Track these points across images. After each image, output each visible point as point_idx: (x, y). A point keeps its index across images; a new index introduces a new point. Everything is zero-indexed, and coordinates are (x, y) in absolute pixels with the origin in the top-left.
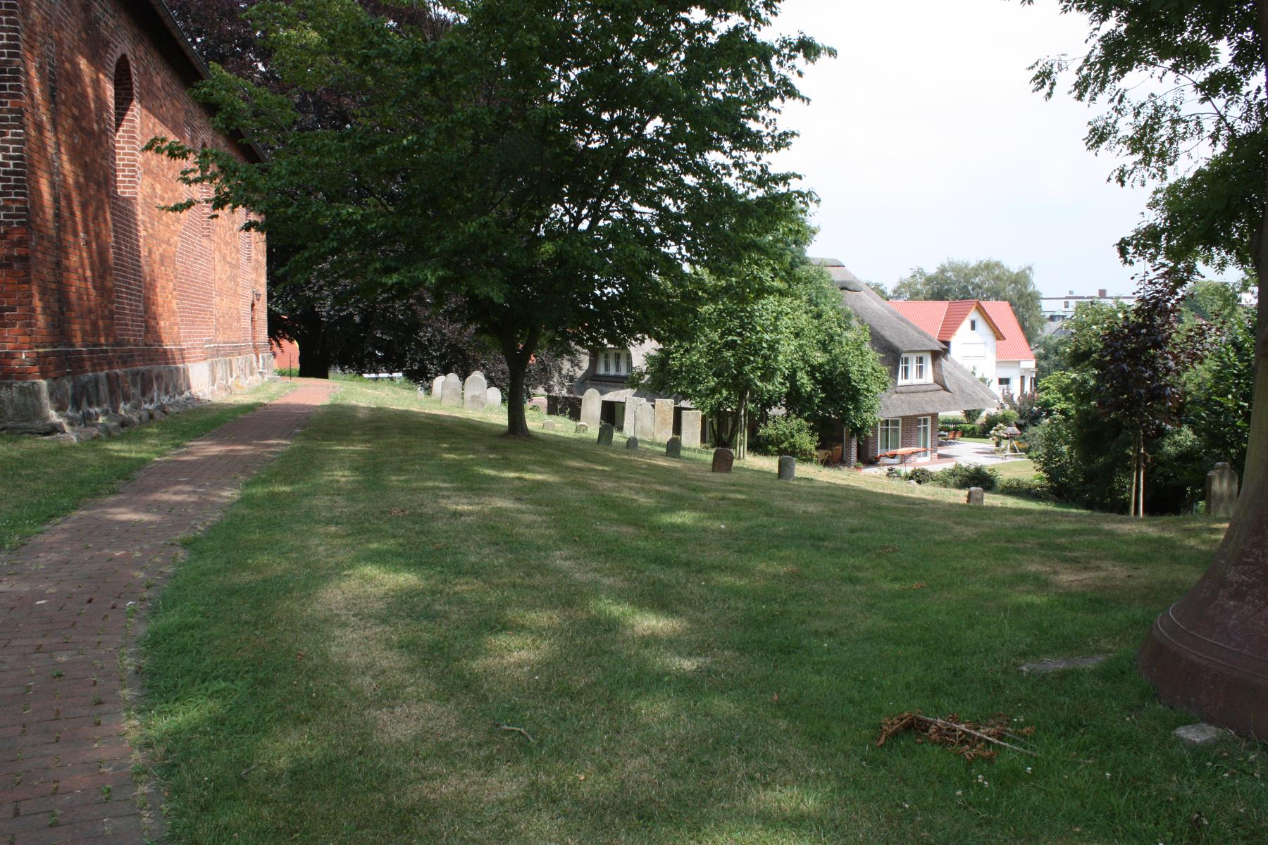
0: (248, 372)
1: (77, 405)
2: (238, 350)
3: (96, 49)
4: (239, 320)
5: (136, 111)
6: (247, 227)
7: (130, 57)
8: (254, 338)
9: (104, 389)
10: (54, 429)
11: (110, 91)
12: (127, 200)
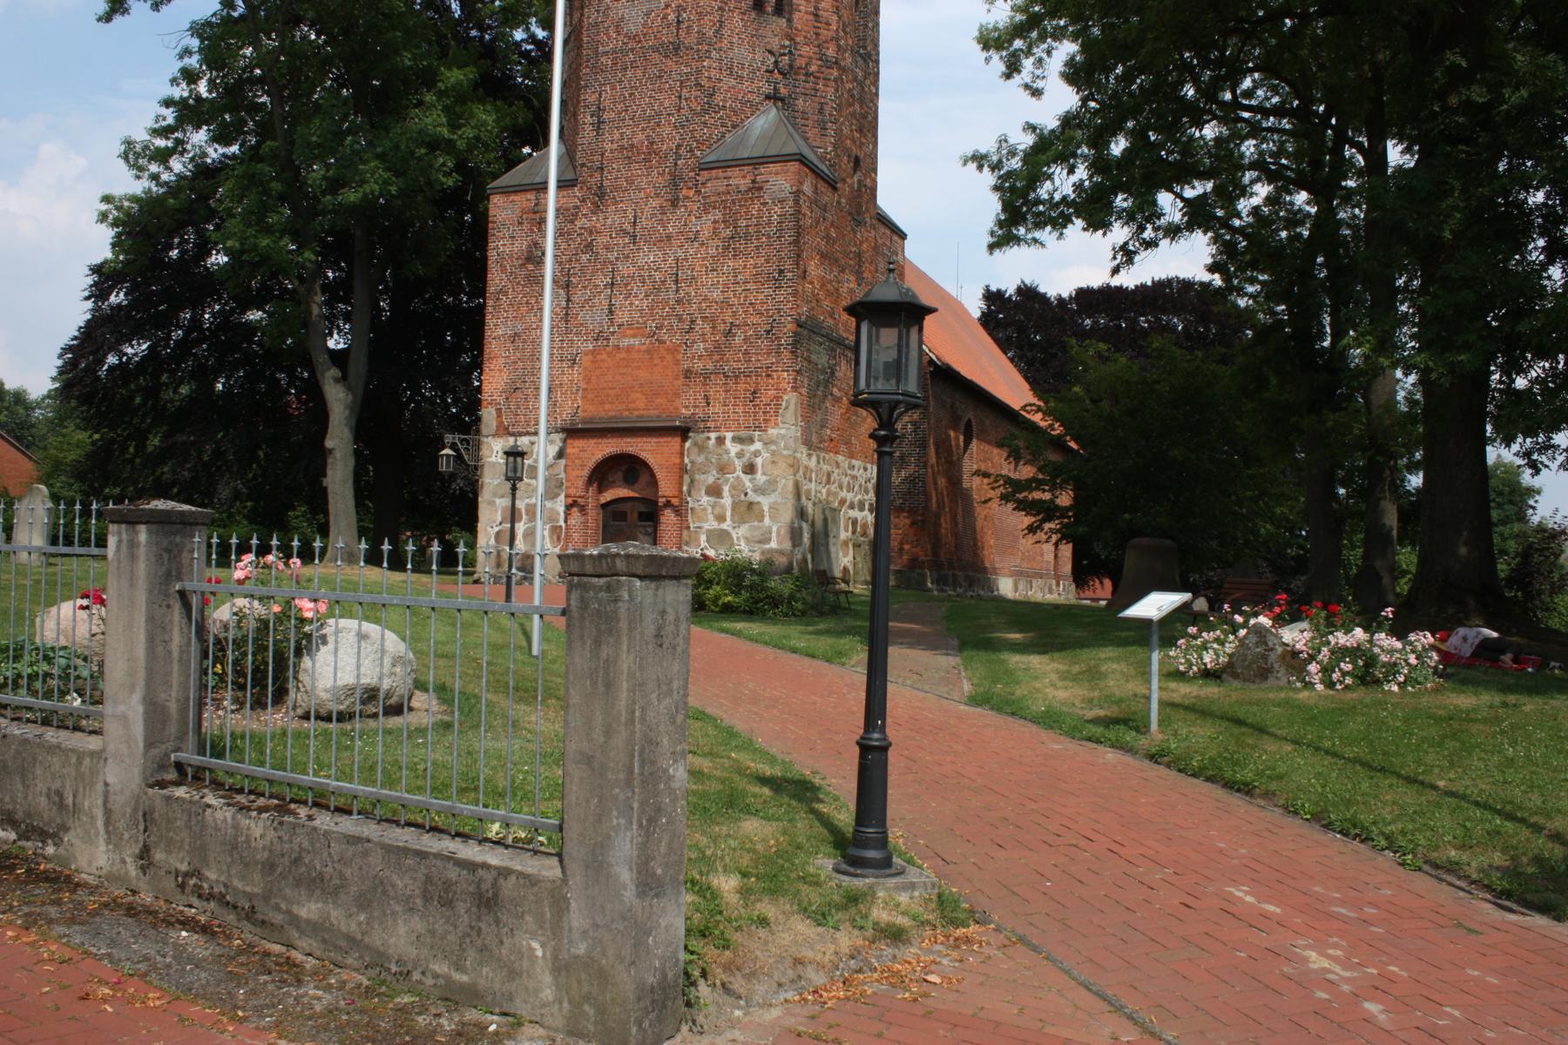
1: (938, 584)
3: (954, 422)
4: (1042, 555)
5: (974, 444)
8: (1056, 569)
9: (951, 580)
10: (930, 590)
11: (962, 438)
12: (967, 489)
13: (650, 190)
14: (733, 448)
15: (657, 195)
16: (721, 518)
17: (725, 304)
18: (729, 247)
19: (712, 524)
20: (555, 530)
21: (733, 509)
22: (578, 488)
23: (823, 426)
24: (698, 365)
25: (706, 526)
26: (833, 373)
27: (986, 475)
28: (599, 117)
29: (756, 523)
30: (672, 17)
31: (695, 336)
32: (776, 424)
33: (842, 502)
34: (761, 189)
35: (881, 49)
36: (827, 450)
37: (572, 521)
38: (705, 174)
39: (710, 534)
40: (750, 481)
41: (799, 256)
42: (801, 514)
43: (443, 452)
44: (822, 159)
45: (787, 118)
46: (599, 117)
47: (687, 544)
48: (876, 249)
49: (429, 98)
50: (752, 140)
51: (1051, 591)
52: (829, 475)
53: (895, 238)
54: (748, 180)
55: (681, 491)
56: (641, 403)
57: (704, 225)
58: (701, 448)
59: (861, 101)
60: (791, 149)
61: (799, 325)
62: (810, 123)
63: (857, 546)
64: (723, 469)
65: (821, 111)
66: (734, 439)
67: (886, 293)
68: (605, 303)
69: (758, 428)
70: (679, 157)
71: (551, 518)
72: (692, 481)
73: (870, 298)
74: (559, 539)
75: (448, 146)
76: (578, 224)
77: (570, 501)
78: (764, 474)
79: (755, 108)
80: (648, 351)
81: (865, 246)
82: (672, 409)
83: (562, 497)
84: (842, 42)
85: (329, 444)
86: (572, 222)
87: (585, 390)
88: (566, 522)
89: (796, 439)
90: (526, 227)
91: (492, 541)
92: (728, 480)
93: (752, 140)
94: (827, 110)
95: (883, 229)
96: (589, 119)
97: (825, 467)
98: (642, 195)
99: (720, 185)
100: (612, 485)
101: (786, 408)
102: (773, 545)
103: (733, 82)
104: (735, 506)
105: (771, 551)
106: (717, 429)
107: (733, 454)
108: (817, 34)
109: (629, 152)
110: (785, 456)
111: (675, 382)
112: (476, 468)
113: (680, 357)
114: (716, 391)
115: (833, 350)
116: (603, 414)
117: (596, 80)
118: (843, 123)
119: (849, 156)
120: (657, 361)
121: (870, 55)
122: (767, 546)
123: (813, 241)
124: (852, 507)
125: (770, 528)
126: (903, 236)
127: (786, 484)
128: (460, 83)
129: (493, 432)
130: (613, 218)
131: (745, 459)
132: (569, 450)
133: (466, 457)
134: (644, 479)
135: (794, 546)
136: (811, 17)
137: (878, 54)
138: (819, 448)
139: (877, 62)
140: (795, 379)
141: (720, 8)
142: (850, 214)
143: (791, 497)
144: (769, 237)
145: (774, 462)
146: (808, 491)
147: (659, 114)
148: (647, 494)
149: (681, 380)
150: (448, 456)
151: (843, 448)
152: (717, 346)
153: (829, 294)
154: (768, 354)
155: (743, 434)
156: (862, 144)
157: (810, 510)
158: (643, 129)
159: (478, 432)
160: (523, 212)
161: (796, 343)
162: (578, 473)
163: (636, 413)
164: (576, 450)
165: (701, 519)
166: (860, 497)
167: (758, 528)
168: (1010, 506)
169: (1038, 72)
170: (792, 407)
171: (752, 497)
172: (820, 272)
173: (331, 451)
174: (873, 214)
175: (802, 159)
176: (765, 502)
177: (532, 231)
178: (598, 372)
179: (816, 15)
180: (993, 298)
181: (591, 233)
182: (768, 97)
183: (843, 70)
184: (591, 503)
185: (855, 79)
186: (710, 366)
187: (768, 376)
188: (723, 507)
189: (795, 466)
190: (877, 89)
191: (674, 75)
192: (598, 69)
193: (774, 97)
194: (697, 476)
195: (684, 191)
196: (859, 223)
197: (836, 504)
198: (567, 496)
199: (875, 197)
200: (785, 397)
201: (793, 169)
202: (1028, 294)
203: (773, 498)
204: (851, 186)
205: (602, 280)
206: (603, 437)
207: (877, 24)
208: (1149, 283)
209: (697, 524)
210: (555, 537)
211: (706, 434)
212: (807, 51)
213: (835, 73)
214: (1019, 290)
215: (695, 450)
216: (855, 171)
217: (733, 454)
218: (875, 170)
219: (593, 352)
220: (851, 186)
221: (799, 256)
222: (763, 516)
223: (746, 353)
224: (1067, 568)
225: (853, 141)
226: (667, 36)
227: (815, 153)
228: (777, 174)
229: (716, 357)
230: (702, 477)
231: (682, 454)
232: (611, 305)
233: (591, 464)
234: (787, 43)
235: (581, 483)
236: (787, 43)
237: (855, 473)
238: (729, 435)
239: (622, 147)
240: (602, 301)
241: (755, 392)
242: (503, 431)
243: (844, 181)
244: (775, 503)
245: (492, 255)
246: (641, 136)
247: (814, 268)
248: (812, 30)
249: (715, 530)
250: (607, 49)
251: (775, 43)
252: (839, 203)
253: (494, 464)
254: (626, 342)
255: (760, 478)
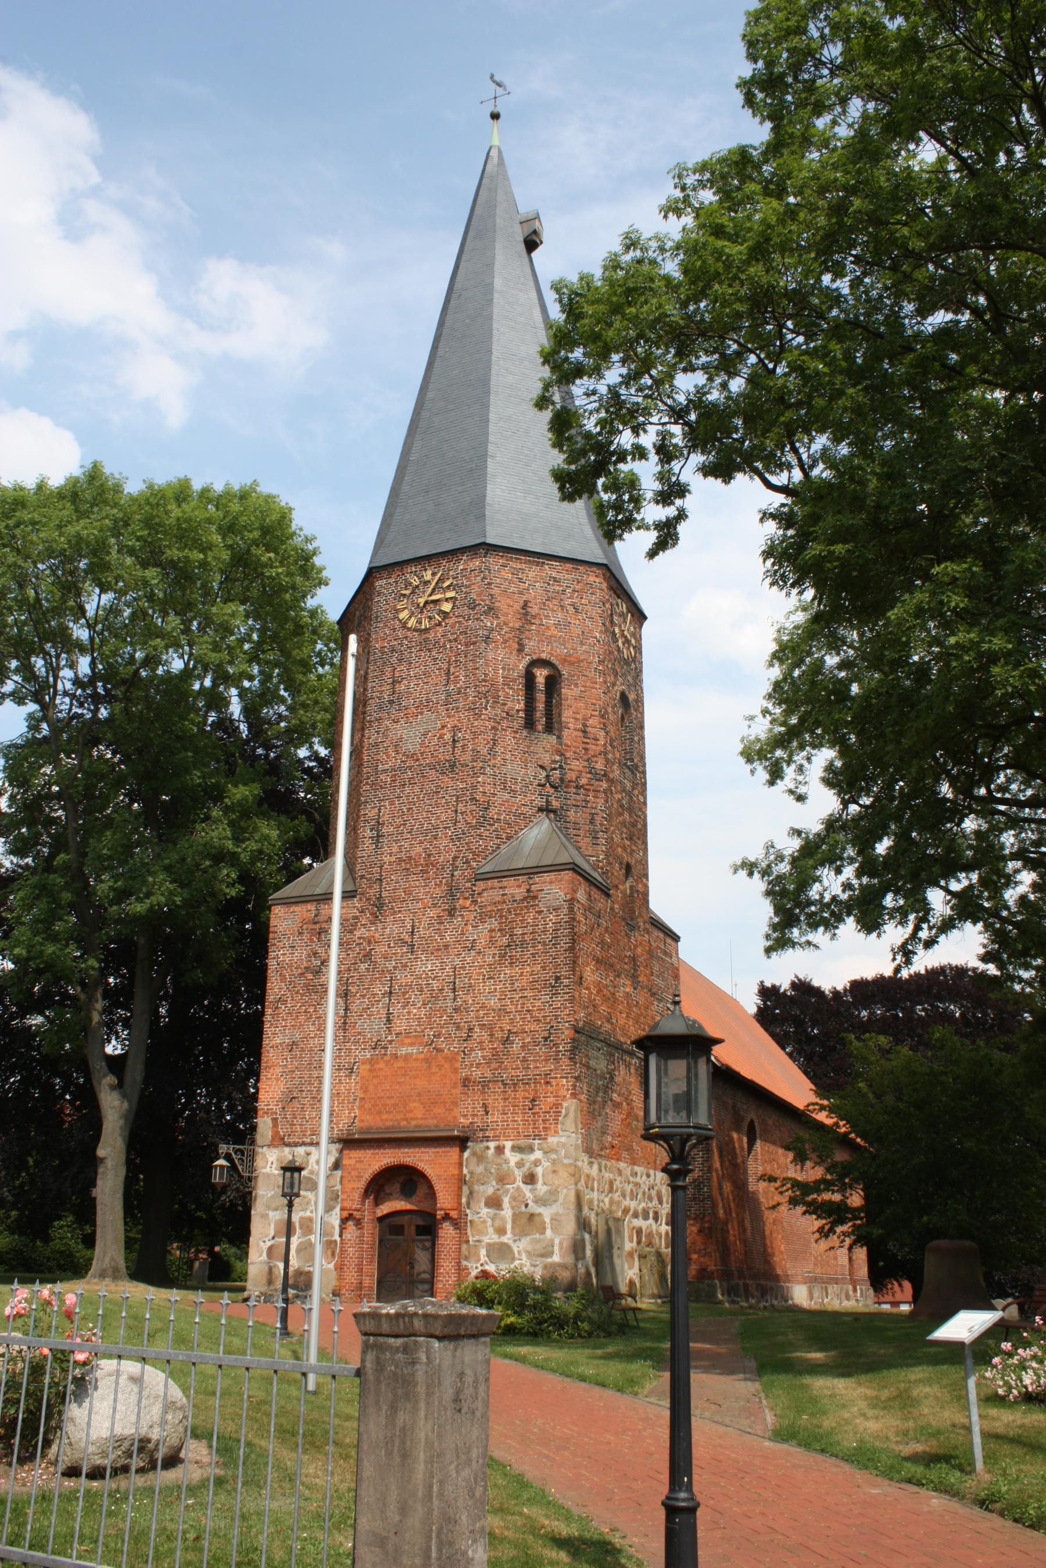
0: (843, 1297)
1: (729, 1295)
2: (836, 1281)
4: (836, 1259)
5: (758, 1145)
6: (804, 1213)
7: (755, 1118)
8: (851, 1273)
10: (721, 1302)
11: (745, 1139)
12: (753, 1193)
13: (428, 901)
14: (512, 1158)
15: (435, 905)
16: (501, 1231)
17: (502, 1011)
18: (506, 956)
19: (491, 1237)
20: (330, 1245)
21: (514, 1221)
22: (354, 1200)
23: (604, 1133)
24: (476, 1074)
25: (486, 1240)
26: (612, 1078)
27: (772, 1179)
28: (378, 831)
29: (537, 1236)
30: (448, 737)
31: (471, 1044)
32: (556, 1132)
33: (626, 1211)
34: (535, 897)
35: (648, 760)
36: (608, 1158)
37: (347, 1235)
38: (481, 885)
39: (491, 1248)
40: (531, 1191)
41: (574, 962)
42: (583, 1224)
43: (218, 1163)
44: (595, 867)
45: (560, 829)
46: (378, 831)
47: (466, 1258)
48: (650, 953)
49: (216, 813)
50: (526, 850)
51: (848, 1298)
52: (611, 1183)
53: (669, 940)
54: (523, 890)
55: (460, 1204)
56: (419, 1113)
57: (481, 934)
58: (481, 1158)
59: (630, 810)
60: (564, 858)
61: (577, 1032)
62: (582, 833)
63: (642, 1257)
64: (503, 1179)
65: (592, 822)
66: (514, 1148)
67: (673, 1027)
68: (383, 1012)
69: (537, 1136)
70: (455, 868)
71: (325, 1232)
72: (471, 1193)
73: (658, 1032)
74: (333, 1254)
75: (232, 859)
76: (358, 933)
77: (345, 1214)
78: (545, 1184)
79: (528, 820)
80: (426, 1060)
81: (639, 950)
82: (450, 1118)
83: (337, 1210)
84: (610, 756)
85: (101, 1152)
86: (351, 932)
87: (362, 1099)
88: (341, 1236)
89: (576, 1147)
90: (306, 936)
91: (264, 1256)
92: (507, 1191)
93: (526, 850)
94: (598, 819)
95: (656, 933)
96: (368, 833)
97: (608, 1175)
98: (420, 905)
99: (495, 895)
100: (389, 1197)
101: (566, 1115)
102: (556, 1258)
103: (507, 796)
104: (515, 1217)
105: (553, 1265)
106: (496, 1138)
107: (512, 1163)
108: (586, 749)
109: (406, 864)
110: (566, 1166)
111: (453, 1091)
112: (250, 1179)
113: (458, 1065)
114: (495, 1100)
115: (611, 1055)
116: (380, 1124)
117: (375, 796)
118: (613, 832)
119: (621, 863)
120: (434, 1069)
121: (636, 767)
122: (549, 1260)
123: (588, 947)
124: (636, 1215)
125: (552, 1241)
126: (676, 938)
127: (567, 1194)
128: (245, 798)
129: (268, 1142)
130: (392, 927)
131: (525, 1169)
132: (345, 1162)
133: (240, 1168)
134: (422, 1190)
135: (577, 1259)
136: (580, 734)
137: (644, 765)
138: (601, 1156)
139: (644, 773)
140: (574, 1086)
141: (493, 728)
142: (624, 919)
143: (573, 1207)
144: (544, 944)
145: (554, 1172)
146: (591, 1201)
147: (436, 828)
148: (425, 1206)
149: (459, 1089)
150: (222, 1167)
151: (625, 1154)
152: (495, 1054)
153: (606, 999)
154: (546, 1061)
155: (522, 1142)
156: (632, 851)
157: (593, 1221)
158: (421, 842)
159: (253, 1142)
160: (304, 922)
161: (574, 1050)
162: (355, 1185)
163: (413, 1123)
164: (352, 1162)
165: (481, 1232)
166: (643, 1205)
167: (540, 1241)
168: (800, 1209)
169: (800, 778)
170: (572, 1115)
171: (533, 1208)
172: (596, 977)
173: (102, 1160)
174: (646, 917)
175: (575, 869)
176: (546, 1213)
177: (312, 940)
178: (375, 1081)
179: (584, 732)
180: (768, 993)
181: (370, 942)
182: (541, 810)
183: (611, 781)
184: (367, 1217)
185: (624, 791)
186: (488, 1074)
187: (547, 1083)
188: (503, 1219)
189: (576, 1174)
190: (645, 798)
191: (450, 791)
192: (376, 786)
193: (546, 810)
194: (476, 1188)
195: (461, 901)
196: (633, 928)
197: (620, 1214)
198: (342, 1209)
199: (646, 901)
200: (565, 1105)
201: (566, 878)
202: (802, 988)
203: (555, 1209)
204: (624, 892)
205: (380, 989)
206: (379, 1147)
207: (642, 738)
208: (923, 972)
209: (477, 1238)
210: (329, 1253)
211: (485, 1144)
212: (576, 765)
213: (605, 785)
214: (793, 985)
215: (475, 1160)
216: (627, 878)
217: (512, 1163)
218: (646, 876)
219: (371, 1062)
220: (624, 892)
221: (574, 962)
222: (545, 1228)
223: (524, 1060)
224: (863, 1271)
225: (624, 848)
226: (445, 754)
227: (588, 861)
228: (551, 883)
229: (494, 1065)
230: (482, 1188)
231: (461, 1165)
232: (389, 1014)
233: (367, 1176)
234: (558, 758)
235: (357, 1196)
236: (558, 758)
237: (638, 1180)
238: (508, 1145)
239: (400, 860)
240: (379, 1009)
241: (534, 1100)
242: (279, 1141)
243: (616, 887)
244: (557, 1214)
245: (272, 964)
246: (419, 849)
247: (590, 974)
248: (581, 746)
249: (495, 1244)
250: (386, 767)
251: (546, 759)
252: (612, 909)
253: (268, 1175)
254: (404, 1051)
255: (541, 1188)
